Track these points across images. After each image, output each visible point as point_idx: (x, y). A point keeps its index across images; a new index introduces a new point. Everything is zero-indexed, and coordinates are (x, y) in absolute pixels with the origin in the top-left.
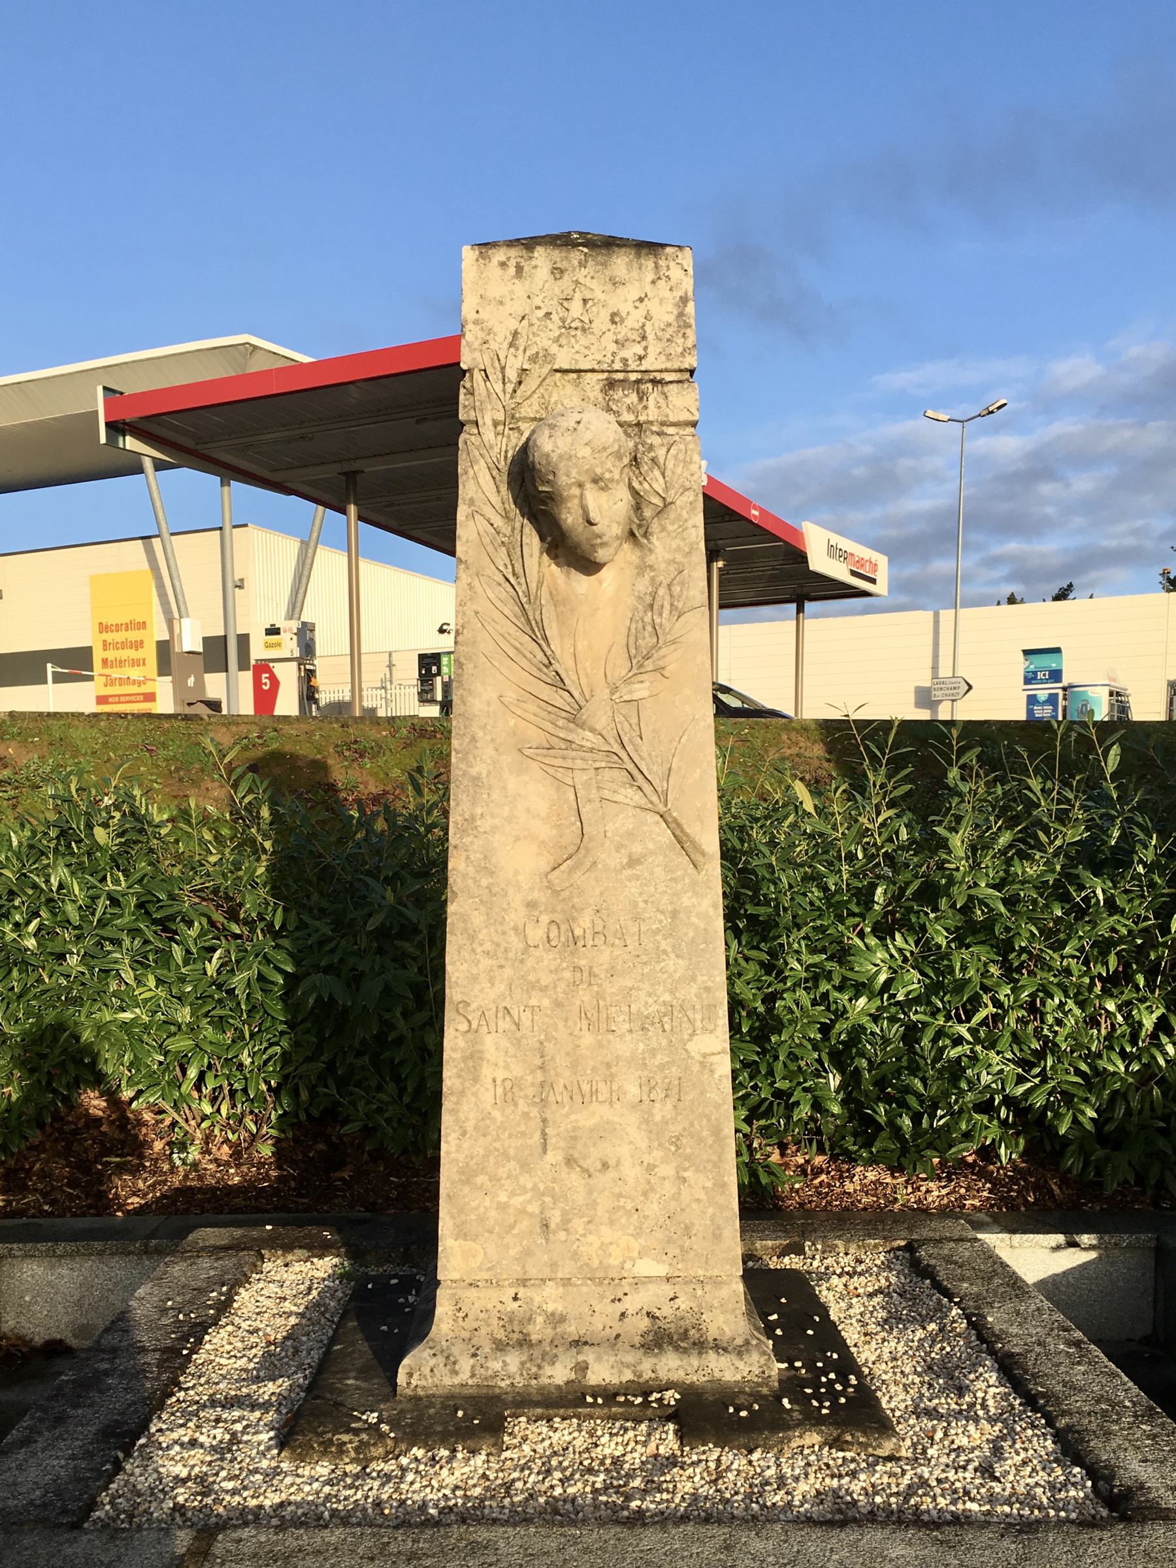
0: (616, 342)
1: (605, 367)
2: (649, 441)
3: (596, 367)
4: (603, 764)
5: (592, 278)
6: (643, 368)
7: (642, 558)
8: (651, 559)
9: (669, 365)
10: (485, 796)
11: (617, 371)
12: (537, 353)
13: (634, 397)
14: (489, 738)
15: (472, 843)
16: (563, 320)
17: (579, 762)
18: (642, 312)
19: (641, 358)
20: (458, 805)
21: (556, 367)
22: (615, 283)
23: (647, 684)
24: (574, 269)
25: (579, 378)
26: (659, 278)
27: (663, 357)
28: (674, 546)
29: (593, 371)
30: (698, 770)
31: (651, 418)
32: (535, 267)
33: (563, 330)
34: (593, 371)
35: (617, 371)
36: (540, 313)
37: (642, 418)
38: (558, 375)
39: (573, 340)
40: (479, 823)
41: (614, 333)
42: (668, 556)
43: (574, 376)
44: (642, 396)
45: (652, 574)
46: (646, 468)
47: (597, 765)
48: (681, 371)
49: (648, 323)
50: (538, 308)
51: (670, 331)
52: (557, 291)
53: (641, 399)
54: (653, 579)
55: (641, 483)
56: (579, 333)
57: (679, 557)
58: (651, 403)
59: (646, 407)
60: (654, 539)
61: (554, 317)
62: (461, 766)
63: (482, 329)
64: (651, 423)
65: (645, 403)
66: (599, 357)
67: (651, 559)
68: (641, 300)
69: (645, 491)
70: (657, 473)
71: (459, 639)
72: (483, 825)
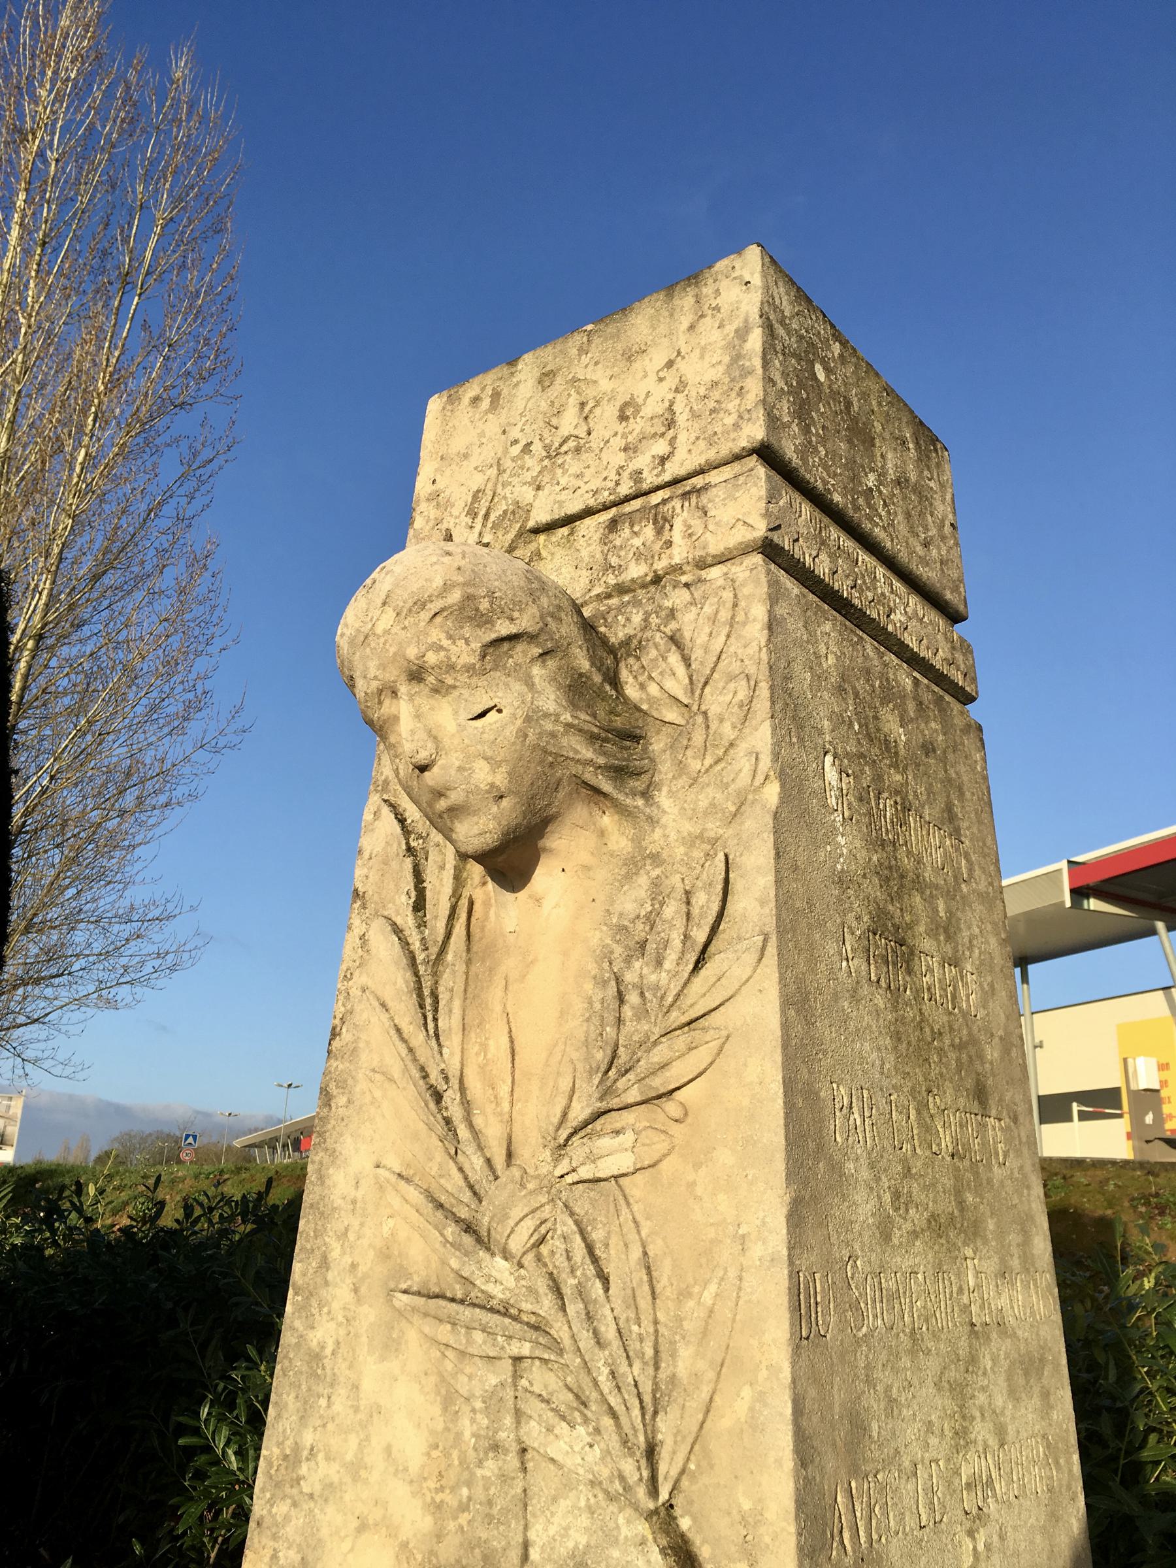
0: (625, 449)
1: (605, 497)
2: (668, 604)
3: (592, 502)
4: (526, 1349)
5: (596, 363)
6: (667, 477)
7: (637, 841)
8: (655, 839)
9: (711, 455)
10: (323, 1402)
11: (627, 499)
12: (505, 512)
13: (649, 531)
14: (347, 1260)
15: (287, 1518)
16: (547, 448)
17: (478, 1336)
18: (671, 381)
19: (663, 460)
20: (279, 1416)
21: (531, 524)
22: (629, 357)
23: (628, 1138)
24: (571, 361)
25: (572, 533)
26: (702, 316)
27: (702, 444)
28: (703, 803)
29: (588, 512)
30: (747, 1392)
31: (677, 560)
32: (517, 384)
33: (546, 462)
34: (588, 512)
35: (627, 499)
36: (516, 450)
37: (660, 566)
38: (542, 538)
39: (559, 471)
40: (304, 1469)
41: (624, 436)
42: (688, 827)
43: (564, 531)
44: (662, 523)
45: (657, 871)
46: (653, 653)
47: (516, 1348)
48: (737, 458)
49: (680, 398)
50: (516, 442)
51: (716, 394)
52: (544, 405)
53: (659, 532)
54: (656, 884)
55: (642, 687)
56: (568, 457)
57: (713, 827)
58: (677, 535)
59: (669, 544)
60: (662, 798)
61: (537, 448)
62: (297, 1324)
63: (438, 504)
64: (677, 569)
65: (666, 535)
66: (595, 484)
67: (655, 839)
68: (670, 364)
69: (651, 700)
70: (674, 658)
71: (336, 1044)
72: (314, 1475)
